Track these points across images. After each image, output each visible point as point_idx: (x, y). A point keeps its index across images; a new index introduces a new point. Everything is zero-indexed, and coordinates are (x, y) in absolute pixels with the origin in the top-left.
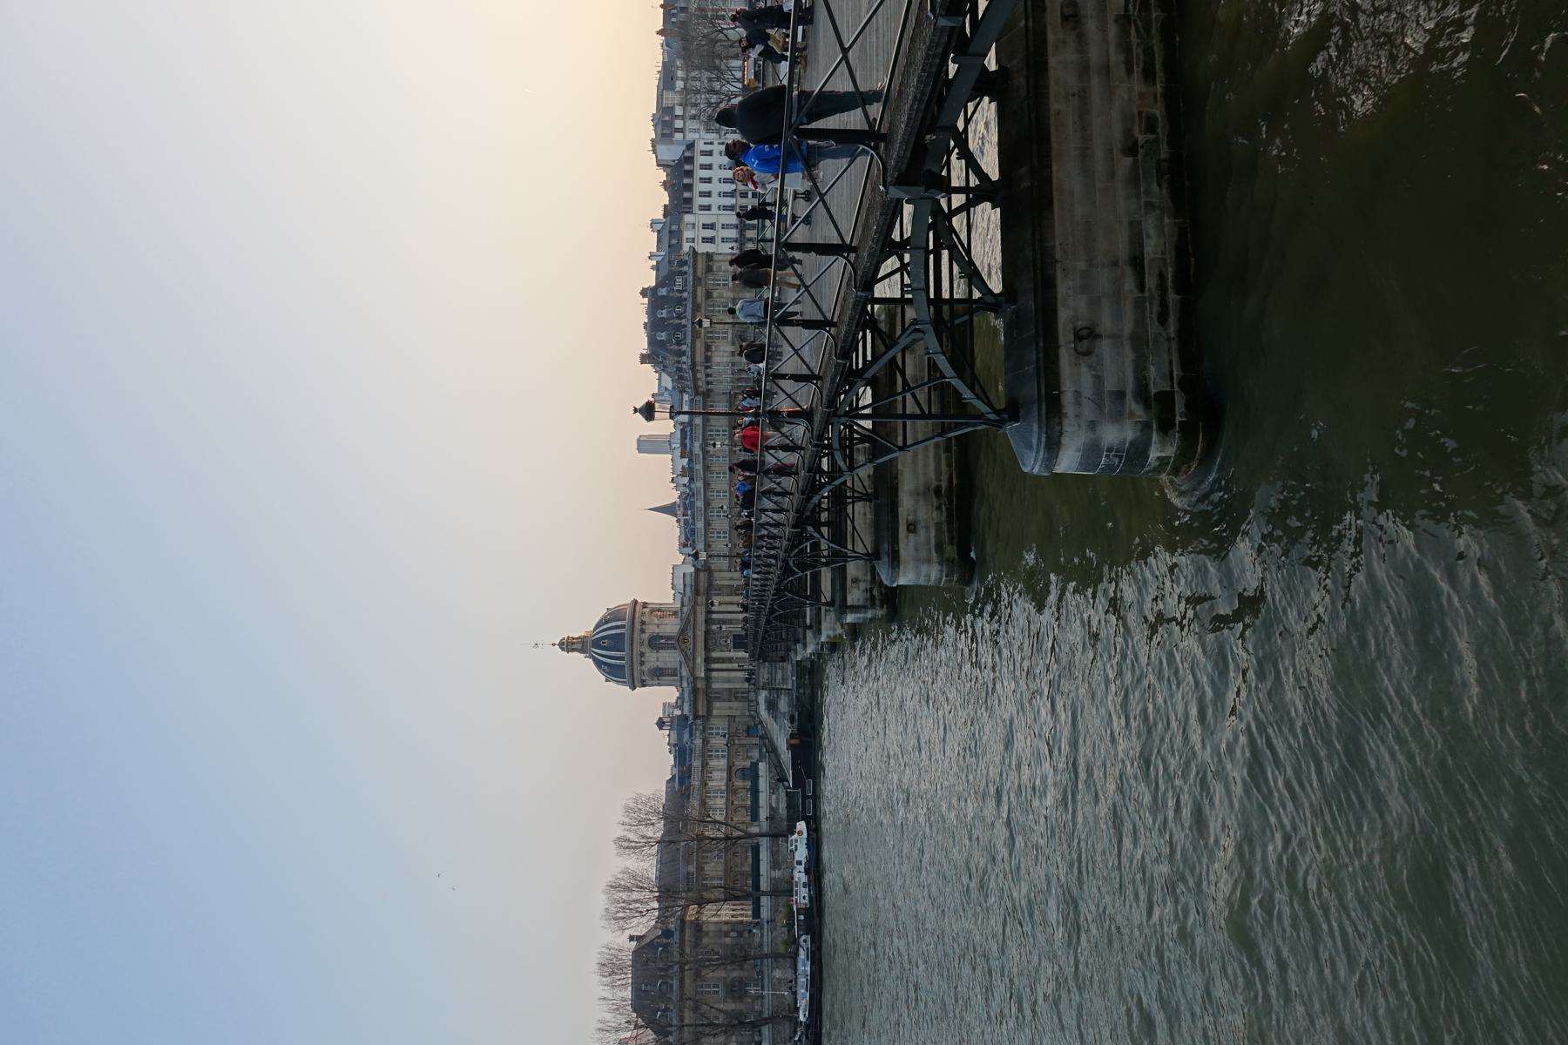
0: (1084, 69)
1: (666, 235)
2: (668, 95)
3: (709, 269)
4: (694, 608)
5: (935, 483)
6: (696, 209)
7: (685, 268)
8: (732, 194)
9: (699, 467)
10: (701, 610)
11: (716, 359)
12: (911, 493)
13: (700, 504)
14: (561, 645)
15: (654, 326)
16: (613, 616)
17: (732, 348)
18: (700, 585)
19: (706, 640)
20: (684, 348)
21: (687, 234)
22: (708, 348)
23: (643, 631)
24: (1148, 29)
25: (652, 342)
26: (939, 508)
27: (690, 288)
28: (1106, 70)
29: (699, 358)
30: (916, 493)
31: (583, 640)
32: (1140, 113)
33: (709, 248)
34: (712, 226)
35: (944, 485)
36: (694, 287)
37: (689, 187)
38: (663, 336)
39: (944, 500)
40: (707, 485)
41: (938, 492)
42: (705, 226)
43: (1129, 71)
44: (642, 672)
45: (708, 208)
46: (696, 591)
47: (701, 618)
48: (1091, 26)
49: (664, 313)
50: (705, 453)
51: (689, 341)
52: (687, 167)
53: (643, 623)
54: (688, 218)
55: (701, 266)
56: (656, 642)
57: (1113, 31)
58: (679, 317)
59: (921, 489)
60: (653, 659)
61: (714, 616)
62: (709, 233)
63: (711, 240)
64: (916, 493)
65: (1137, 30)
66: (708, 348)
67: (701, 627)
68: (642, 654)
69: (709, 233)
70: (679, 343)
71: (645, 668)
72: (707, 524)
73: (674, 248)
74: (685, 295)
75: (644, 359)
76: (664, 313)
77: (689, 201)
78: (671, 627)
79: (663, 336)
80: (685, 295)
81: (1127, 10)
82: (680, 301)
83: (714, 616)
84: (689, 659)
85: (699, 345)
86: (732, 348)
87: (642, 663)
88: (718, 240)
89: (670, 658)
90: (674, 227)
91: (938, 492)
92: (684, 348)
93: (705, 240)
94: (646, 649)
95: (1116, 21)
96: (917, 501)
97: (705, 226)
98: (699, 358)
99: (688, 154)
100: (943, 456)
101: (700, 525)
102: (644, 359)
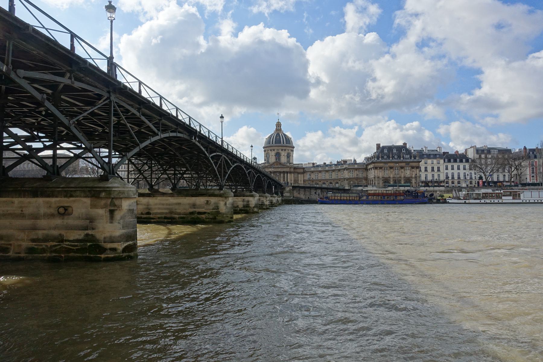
0: (35, 217)
1: (436, 153)
2: (496, 152)
3: (413, 167)
4: (288, 167)
5: (151, 212)
6: (446, 164)
7: (413, 158)
8: (453, 178)
9: (339, 167)
10: (288, 170)
11: (376, 171)
12: (148, 202)
13: (327, 168)
14: (278, 122)
15: (390, 148)
16: (288, 140)
17: (381, 177)
18: (299, 170)
19: (278, 172)
20: (380, 159)
21: (435, 161)
22: (381, 168)
23: (282, 150)
24: (55, 251)
25: (384, 147)
27: (404, 160)
28: (34, 228)
29: (377, 165)
30: (148, 205)
31: (281, 129)
32: (11, 245)
33: (423, 169)
34: (439, 170)
35: (151, 216)
36: (405, 162)
37: (455, 161)
38: (386, 151)
39: (145, 216)
40: (333, 171)
41: (148, 213)
42: (439, 168)
43: (33, 240)
44: (268, 151)
45: (447, 169)
46: (295, 168)
47: (285, 170)
48: (58, 221)
49: (395, 151)
50: (344, 169)
51: (383, 161)
52: (464, 160)
53: (285, 150)
54: (442, 161)
55: (414, 164)
56: (278, 155)
57: (55, 233)
58: (393, 157)
59: (150, 207)
60: (273, 153)
61: (286, 174)
62: (436, 169)
63: (433, 170)
64: (148, 205)
65: (55, 246)
66: (381, 168)
67: (282, 170)
68: (274, 150)
69: (436, 169)
70: (382, 157)
71: (269, 152)
72: (320, 172)
73: (429, 156)
74: (402, 159)
75: (378, 146)
76: (395, 151)
77: (449, 161)
78: (283, 159)
79: (386, 151)
80: (402, 159)
81: (66, 241)
82: (399, 157)
83: (286, 174)
84: (271, 166)
85: (381, 165)
86: (381, 177)
87: (271, 150)
88: (433, 173)
89: (273, 160)
90: (438, 156)
91: (148, 213)
92: (380, 159)
93: (433, 168)
95: (60, 235)
96: (145, 205)
97: (439, 168)
98: (377, 165)
99: (470, 160)
100: (163, 216)
101: (320, 169)
102: (378, 146)
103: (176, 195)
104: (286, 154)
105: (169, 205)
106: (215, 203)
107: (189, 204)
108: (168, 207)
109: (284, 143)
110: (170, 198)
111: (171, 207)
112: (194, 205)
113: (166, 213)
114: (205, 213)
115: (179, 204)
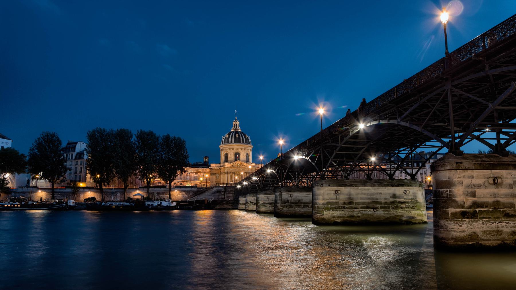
12: (350, 192)
23: (242, 149)
26: (344, 203)
53: (245, 149)
59: (352, 196)
68: (233, 149)
71: (228, 150)
87: (230, 149)
94: (235, 151)
96: (347, 195)
103: (377, 185)
104: (245, 154)
105: (371, 194)
106: (413, 193)
107: (389, 194)
108: (369, 196)
109: (243, 142)
110: (371, 188)
111: (372, 196)
112: (394, 196)
113: (369, 203)
114: (404, 202)
115: (380, 194)
